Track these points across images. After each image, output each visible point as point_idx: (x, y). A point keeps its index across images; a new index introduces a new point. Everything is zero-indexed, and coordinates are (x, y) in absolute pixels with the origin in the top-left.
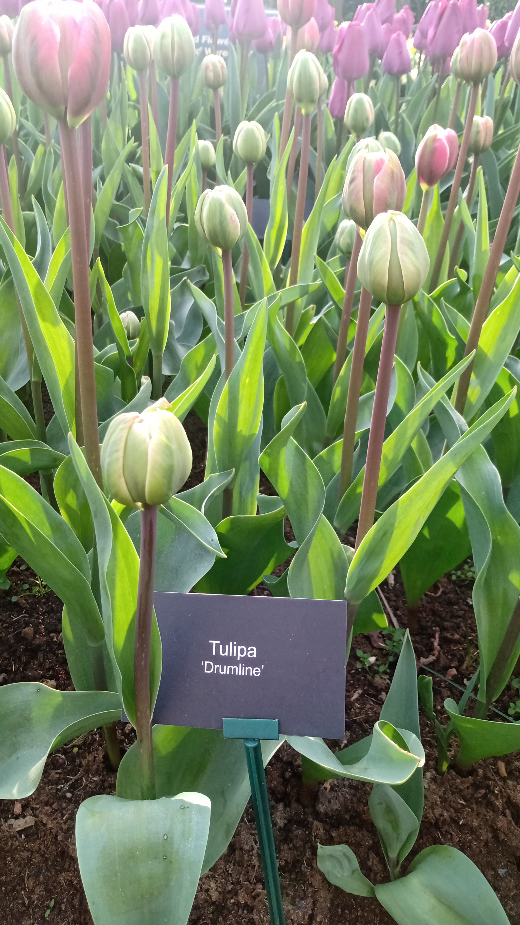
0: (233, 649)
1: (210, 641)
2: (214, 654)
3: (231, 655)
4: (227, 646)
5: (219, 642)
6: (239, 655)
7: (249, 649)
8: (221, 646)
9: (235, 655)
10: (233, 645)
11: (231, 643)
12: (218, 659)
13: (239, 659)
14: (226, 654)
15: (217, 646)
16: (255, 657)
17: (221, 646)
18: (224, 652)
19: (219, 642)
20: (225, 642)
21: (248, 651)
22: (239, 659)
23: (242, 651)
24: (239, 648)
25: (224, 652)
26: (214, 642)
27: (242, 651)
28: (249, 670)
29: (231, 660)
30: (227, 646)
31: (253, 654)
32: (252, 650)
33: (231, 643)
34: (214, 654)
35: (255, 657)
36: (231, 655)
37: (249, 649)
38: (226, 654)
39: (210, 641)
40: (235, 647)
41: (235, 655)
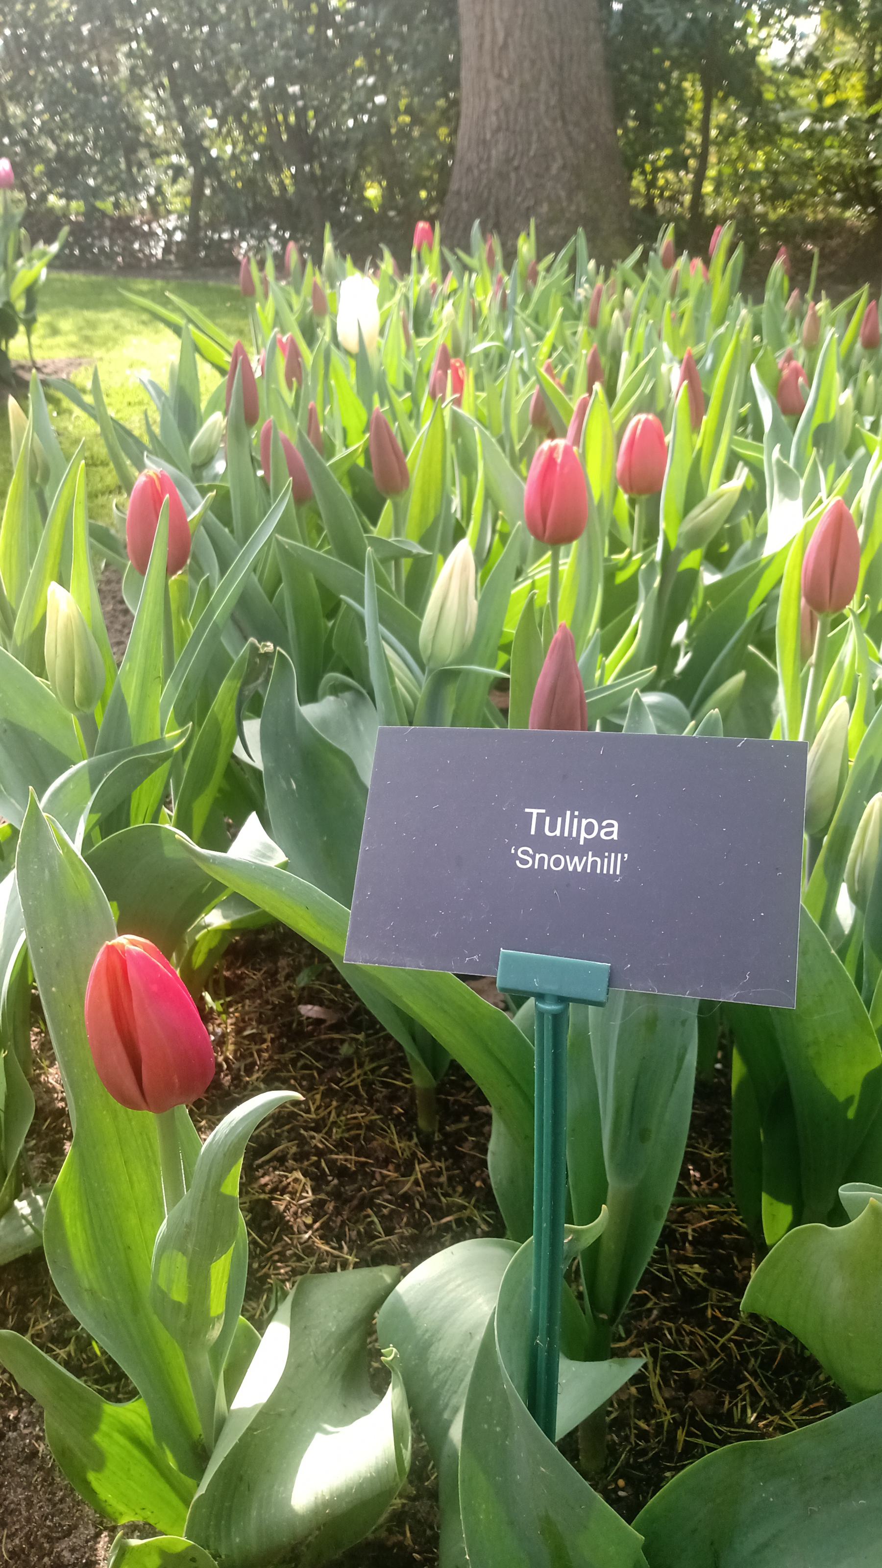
0: (573, 826)
1: (527, 810)
2: (533, 832)
3: (566, 834)
4: (560, 819)
5: (543, 811)
6: (583, 834)
7: (604, 824)
8: (548, 819)
9: (574, 835)
10: (572, 817)
11: (568, 813)
12: (542, 844)
13: (582, 843)
14: (558, 833)
15: (541, 818)
16: (616, 838)
17: (548, 819)
18: (552, 830)
19: (543, 811)
20: (555, 812)
21: (601, 828)
22: (582, 843)
23: (589, 829)
24: (584, 822)
25: (552, 830)
26: (535, 812)
27: (589, 829)
28: (542, 860)
29: (569, 846)
30: (560, 819)
31: (611, 833)
32: (612, 826)
33: (568, 813)
34: (533, 832)
35: (616, 838)
36: (566, 834)
37: (604, 824)
38: (558, 833)
39: (527, 810)
40: (576, 820)
41: (574, 835)
